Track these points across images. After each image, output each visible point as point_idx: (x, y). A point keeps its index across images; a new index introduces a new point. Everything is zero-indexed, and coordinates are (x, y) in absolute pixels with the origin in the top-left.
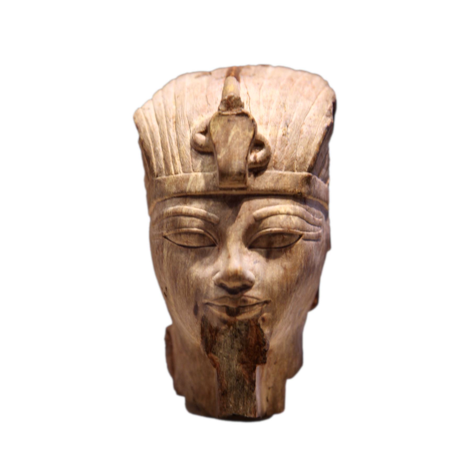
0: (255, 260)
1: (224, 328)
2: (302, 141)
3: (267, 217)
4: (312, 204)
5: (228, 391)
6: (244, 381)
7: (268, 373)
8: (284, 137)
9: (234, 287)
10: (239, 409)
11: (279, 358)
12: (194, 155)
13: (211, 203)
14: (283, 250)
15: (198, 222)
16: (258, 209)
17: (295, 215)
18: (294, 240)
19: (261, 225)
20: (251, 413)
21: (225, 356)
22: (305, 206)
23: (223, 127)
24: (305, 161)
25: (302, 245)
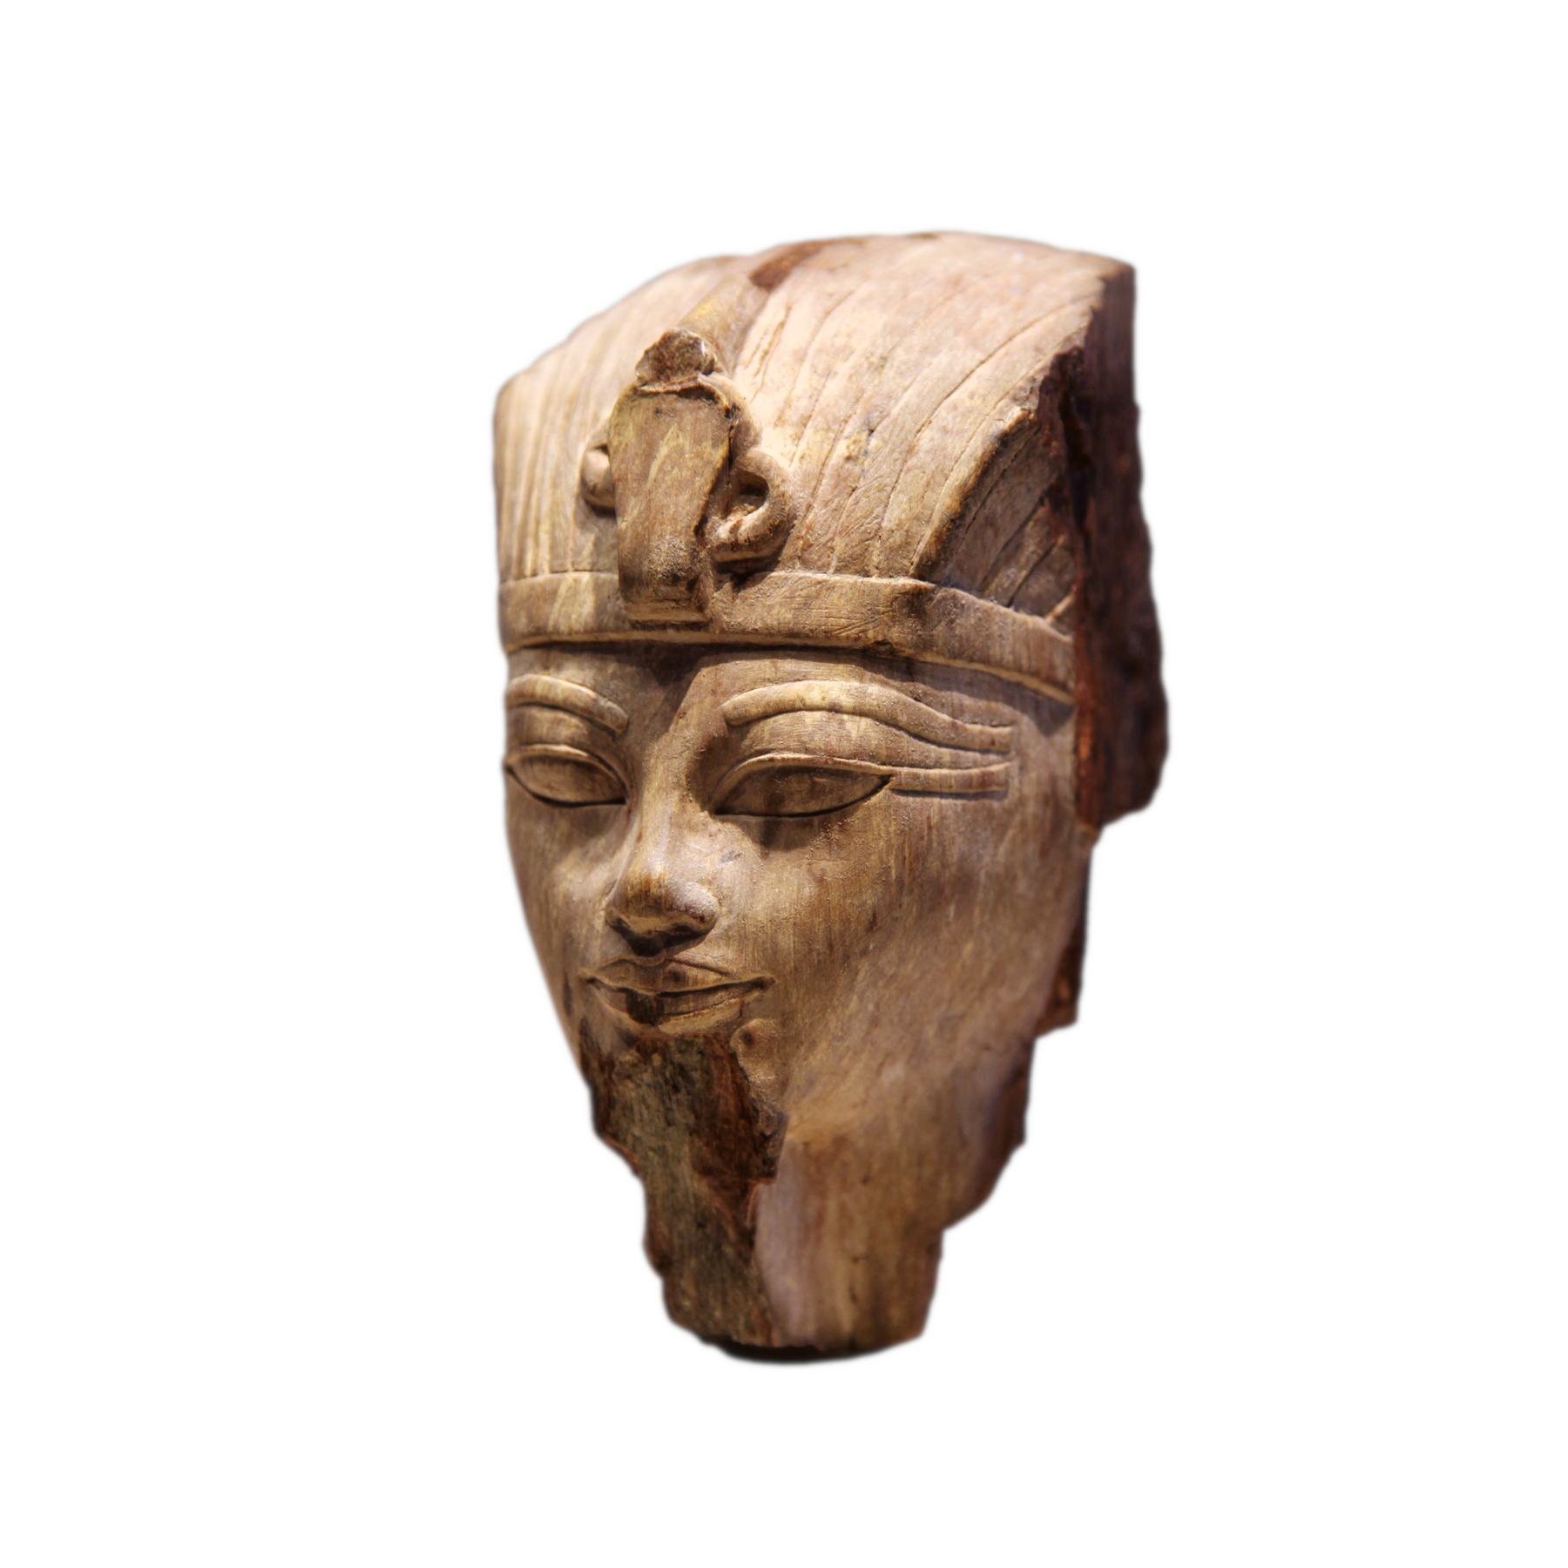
0: (726, 851)
1: (628, 1057)
2: (909, 477)
3: (766, 716)
4: (945, 679)
5: (675, 1258)
6: (720, 1229)
7: (843, 1209)
8: (848, 466)
9: (650, 932)
10: (711, 1316)
11: (876, 1166)
12: (582, 517)
13: (612, 667)
14: (816, 820)
15: (571, 726)
16: (741, 691)
18: (860, 794)
19: (747, 742)
20: (751, 1330)
21: (651, 1149)
22: (909, 686)
23: (642, 431)
24: (906, 544)
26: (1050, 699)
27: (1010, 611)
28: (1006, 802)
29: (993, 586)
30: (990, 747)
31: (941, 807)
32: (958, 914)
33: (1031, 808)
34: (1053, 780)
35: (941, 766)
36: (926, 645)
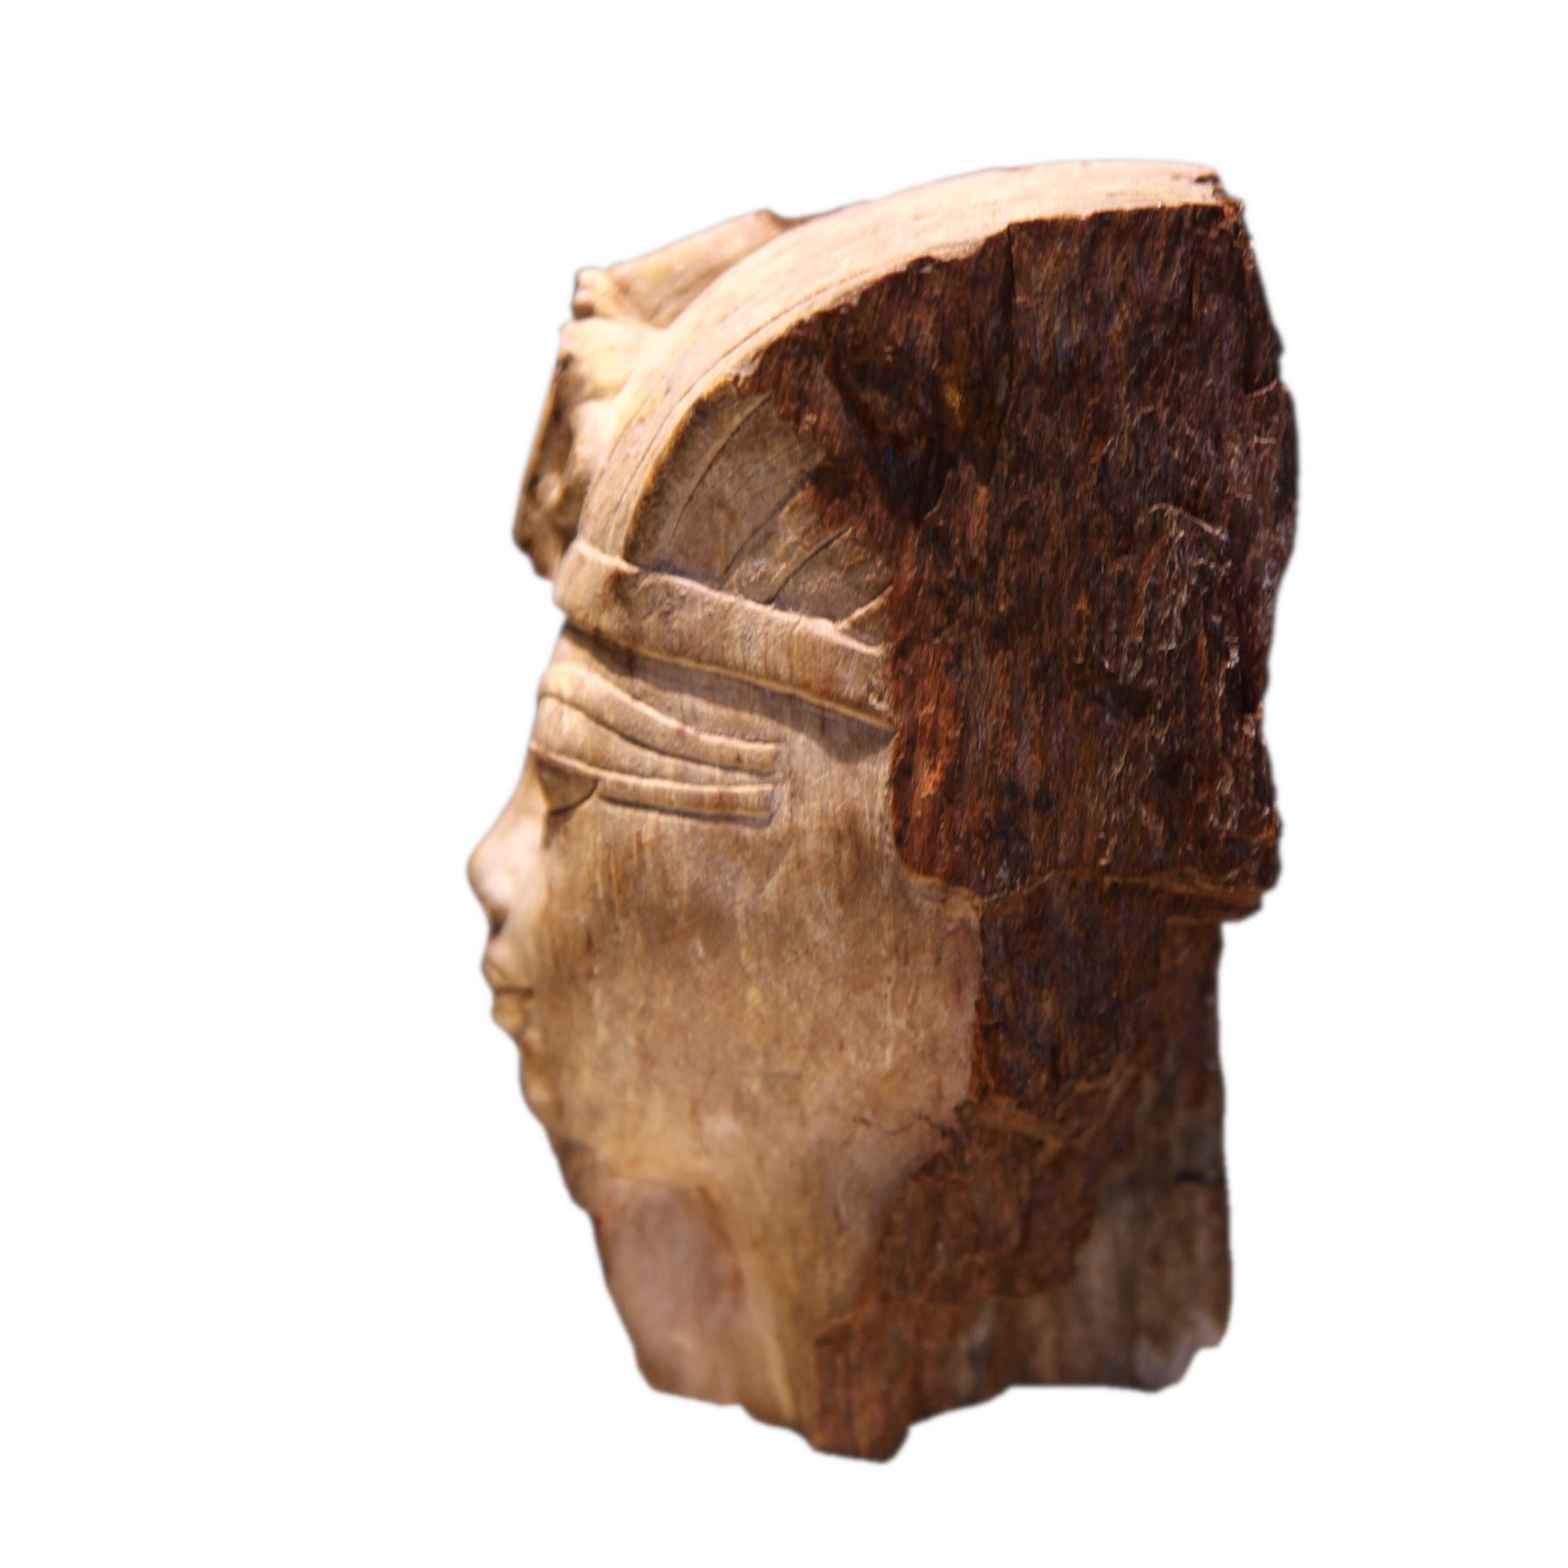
17: (576, 705)
18: (577, 796)
22: (626, 681)
25: (595, 816)
26: (849, 720)
27: (769, 611)
28: (768, 831)
29: (734, 578)
30: (734, 764)
31: (658, 827)
32: (714, 953)
33: (811, 844)
34: (852, 818)
35: (664, 777)
36: (637, 636)
